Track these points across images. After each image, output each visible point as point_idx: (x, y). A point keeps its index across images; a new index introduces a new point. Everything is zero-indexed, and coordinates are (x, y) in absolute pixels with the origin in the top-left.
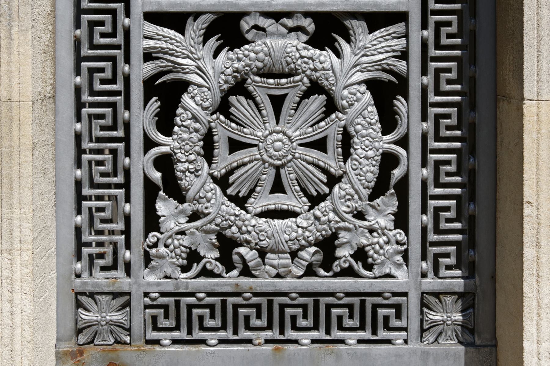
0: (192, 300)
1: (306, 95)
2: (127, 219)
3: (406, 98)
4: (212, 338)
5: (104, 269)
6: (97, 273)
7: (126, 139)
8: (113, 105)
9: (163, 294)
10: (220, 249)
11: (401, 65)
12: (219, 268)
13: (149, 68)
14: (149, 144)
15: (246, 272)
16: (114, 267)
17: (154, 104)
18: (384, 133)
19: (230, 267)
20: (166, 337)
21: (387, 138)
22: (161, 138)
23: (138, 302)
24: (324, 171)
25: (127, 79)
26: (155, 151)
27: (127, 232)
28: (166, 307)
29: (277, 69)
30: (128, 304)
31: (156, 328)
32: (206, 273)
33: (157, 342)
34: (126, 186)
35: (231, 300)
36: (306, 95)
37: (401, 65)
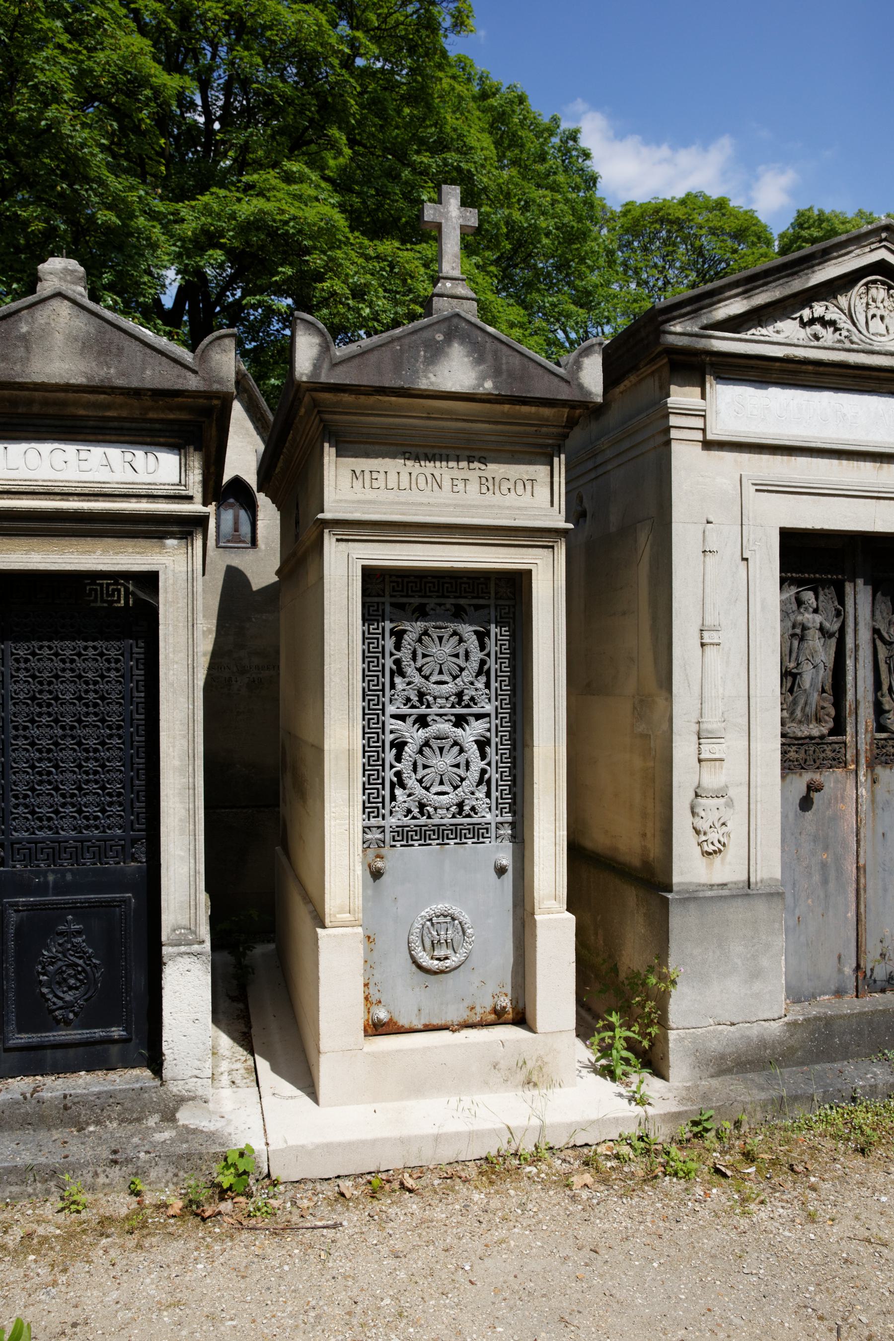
0: (408, 829)
1: (452, 746)
2: (383, 797)
3: (490, 746)
4: (416, 843)
5: (374, 817)
6: (372, 819)
7: (383, 765)
8: (378, 752)
9: (397, 827)
10: (419, 808)
11: (488, 734)
12: (419, 816)
13: (392, 737)
14: (392, 767)
15: (429, 817)
16: (378, 817)
17: (394, 751)
18: (482, 760)
19: (423, 815)
20: (398, 844)
21: (483, 762)
22: (397, 764)
23: (387, 830)
24: (459, 776)
25: (383, 741)
26: (394, 770)
27: (383, 802)
28: (398, 832)
29: (441, 736)
30: (384, 831)
31: (394, 840)
32: (414, 818)
33: (394, 846)
34: (383, 784)
35: (423, 828)
36: (452, 746)
37: (488, 734)
